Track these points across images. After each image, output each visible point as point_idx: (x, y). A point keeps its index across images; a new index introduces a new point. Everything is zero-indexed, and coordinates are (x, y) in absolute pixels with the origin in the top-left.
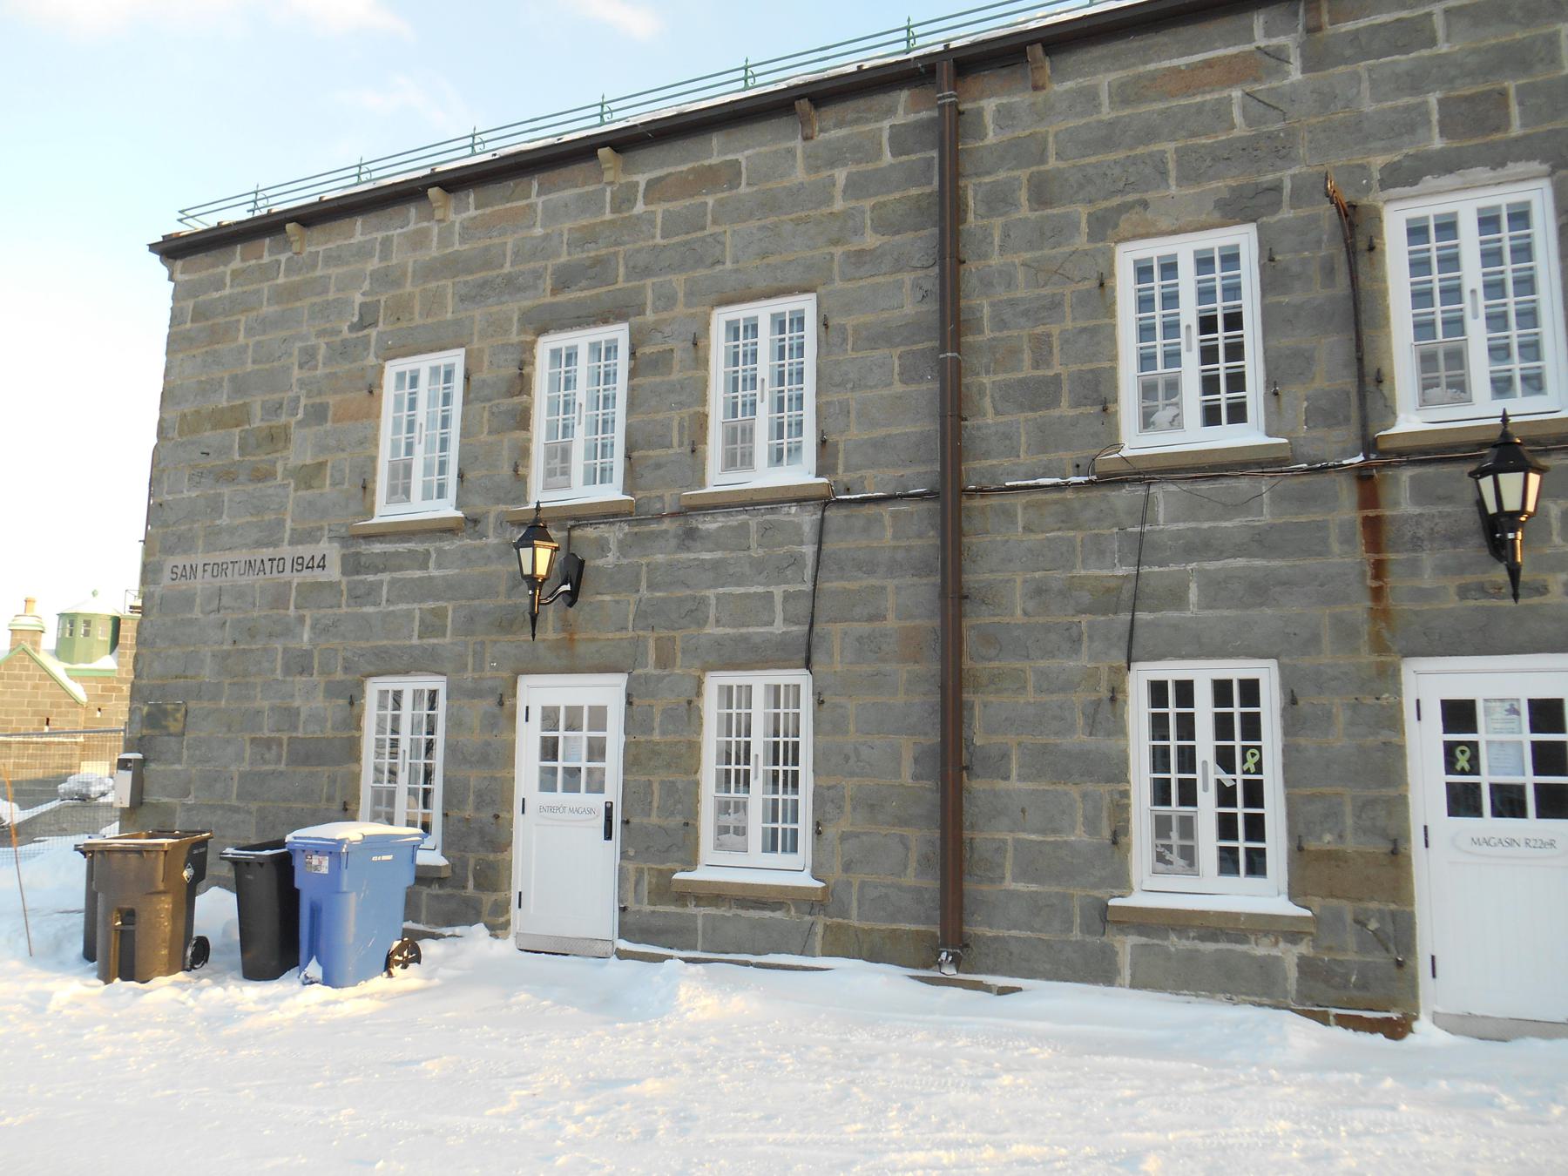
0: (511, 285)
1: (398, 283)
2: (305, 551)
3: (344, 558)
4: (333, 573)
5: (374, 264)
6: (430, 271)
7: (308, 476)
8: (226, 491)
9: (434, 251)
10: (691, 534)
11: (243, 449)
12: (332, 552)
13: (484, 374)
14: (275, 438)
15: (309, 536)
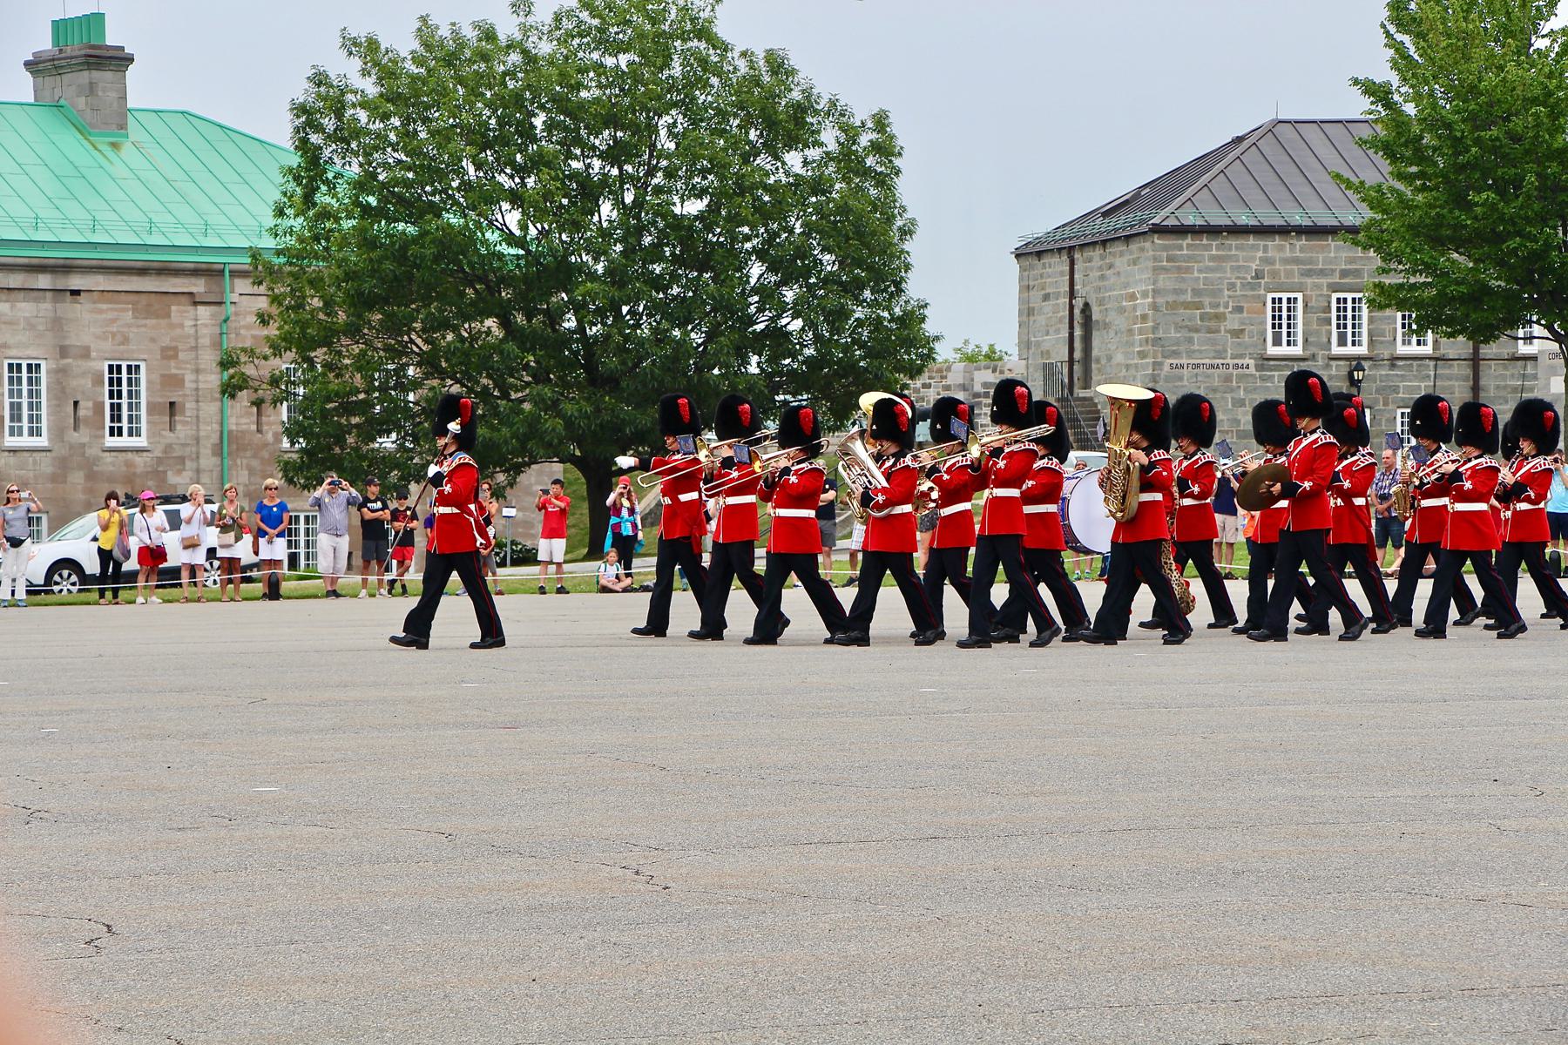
0: (1322, 273)
1: (1273, 263)
2: (1240, 362)
3: (1256, 366)
4: (1252, 370)
5: (1260, 254)
6: (1286, 261)
7: (1237, 333)
8: (1196, 336)
9: (1288, 254)
10: (1393, 366)
11: (1202, 319)
12: (1252, 362)
13: (1312, 304)
14: (1219, 317)
15: (1241, 356)
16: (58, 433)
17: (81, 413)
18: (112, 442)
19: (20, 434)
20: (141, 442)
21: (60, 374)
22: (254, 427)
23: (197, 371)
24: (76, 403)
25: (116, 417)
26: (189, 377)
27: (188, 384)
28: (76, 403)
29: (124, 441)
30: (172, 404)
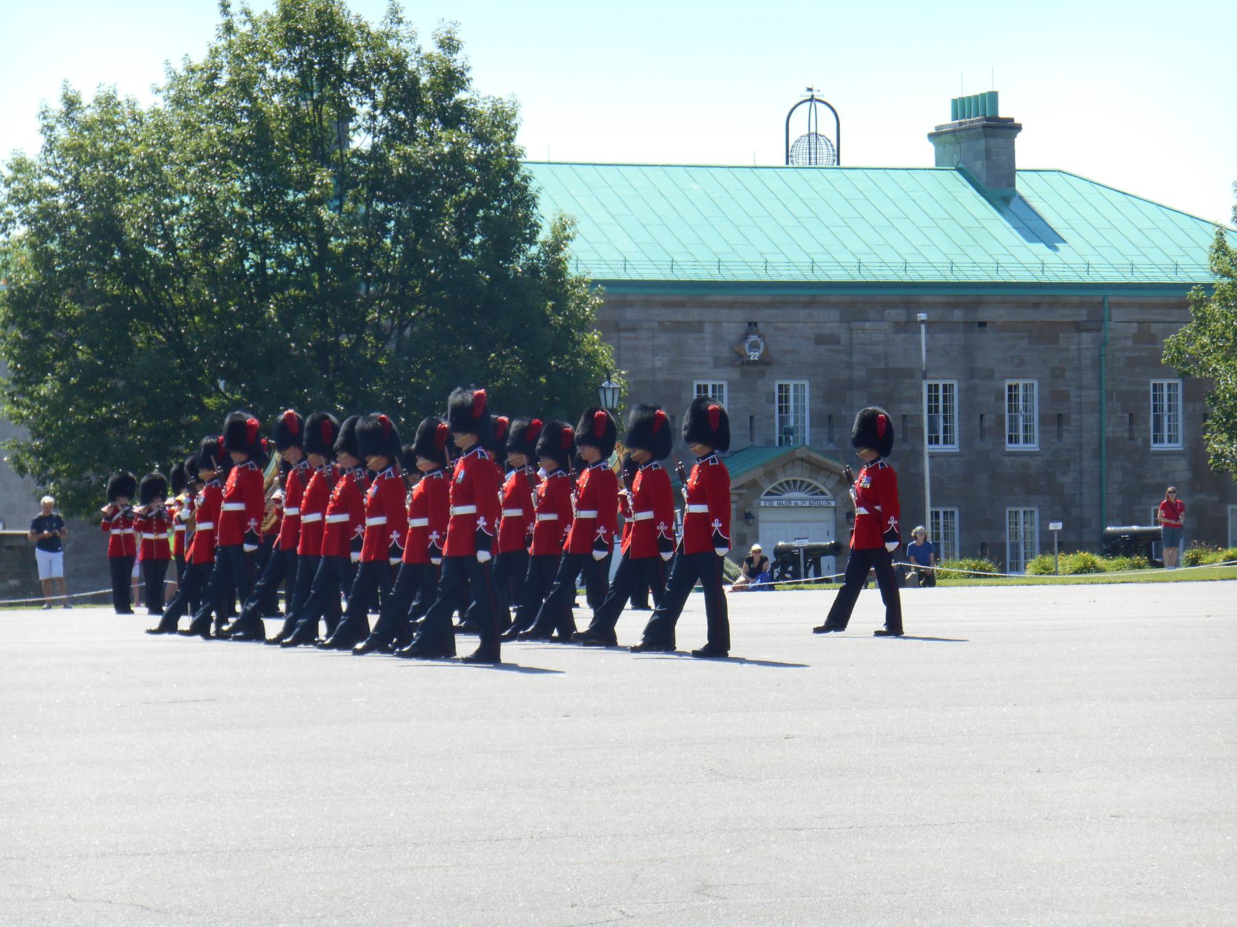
16: (966, 442)
17: (987, 424)
18: (1010, 447)
19: (937, 442)
20: (1034, 447)
21: (969, 393)
22: (1126, 434)
23: (1080, 388)
24: (982, 416)
25: (1014, 428)
26: (1073, 393)
27: (1073, 399)
28: (982, 416)
29: (1021, 446)
30: (1059, 416)
